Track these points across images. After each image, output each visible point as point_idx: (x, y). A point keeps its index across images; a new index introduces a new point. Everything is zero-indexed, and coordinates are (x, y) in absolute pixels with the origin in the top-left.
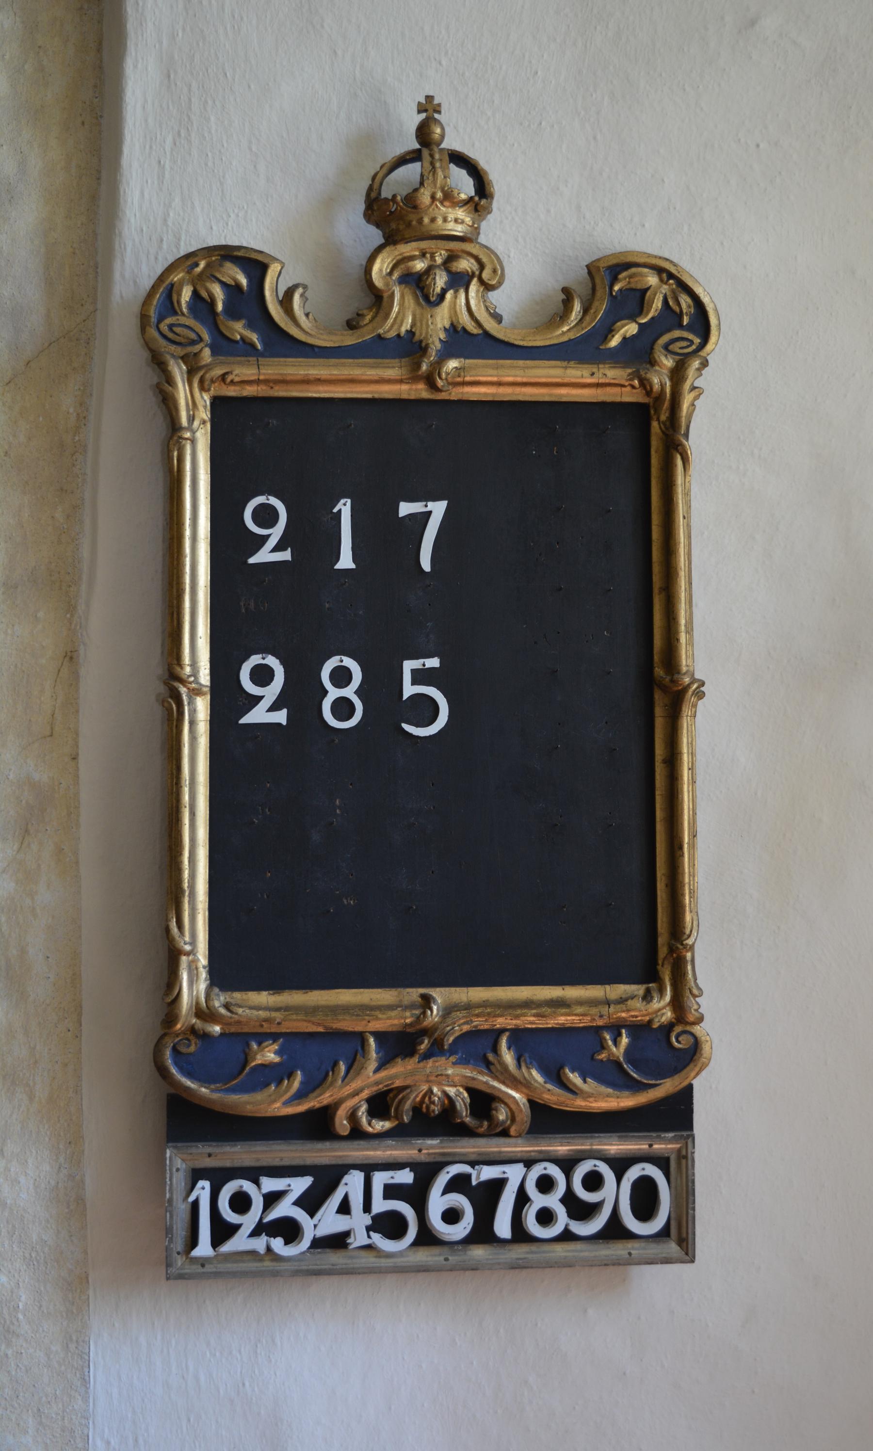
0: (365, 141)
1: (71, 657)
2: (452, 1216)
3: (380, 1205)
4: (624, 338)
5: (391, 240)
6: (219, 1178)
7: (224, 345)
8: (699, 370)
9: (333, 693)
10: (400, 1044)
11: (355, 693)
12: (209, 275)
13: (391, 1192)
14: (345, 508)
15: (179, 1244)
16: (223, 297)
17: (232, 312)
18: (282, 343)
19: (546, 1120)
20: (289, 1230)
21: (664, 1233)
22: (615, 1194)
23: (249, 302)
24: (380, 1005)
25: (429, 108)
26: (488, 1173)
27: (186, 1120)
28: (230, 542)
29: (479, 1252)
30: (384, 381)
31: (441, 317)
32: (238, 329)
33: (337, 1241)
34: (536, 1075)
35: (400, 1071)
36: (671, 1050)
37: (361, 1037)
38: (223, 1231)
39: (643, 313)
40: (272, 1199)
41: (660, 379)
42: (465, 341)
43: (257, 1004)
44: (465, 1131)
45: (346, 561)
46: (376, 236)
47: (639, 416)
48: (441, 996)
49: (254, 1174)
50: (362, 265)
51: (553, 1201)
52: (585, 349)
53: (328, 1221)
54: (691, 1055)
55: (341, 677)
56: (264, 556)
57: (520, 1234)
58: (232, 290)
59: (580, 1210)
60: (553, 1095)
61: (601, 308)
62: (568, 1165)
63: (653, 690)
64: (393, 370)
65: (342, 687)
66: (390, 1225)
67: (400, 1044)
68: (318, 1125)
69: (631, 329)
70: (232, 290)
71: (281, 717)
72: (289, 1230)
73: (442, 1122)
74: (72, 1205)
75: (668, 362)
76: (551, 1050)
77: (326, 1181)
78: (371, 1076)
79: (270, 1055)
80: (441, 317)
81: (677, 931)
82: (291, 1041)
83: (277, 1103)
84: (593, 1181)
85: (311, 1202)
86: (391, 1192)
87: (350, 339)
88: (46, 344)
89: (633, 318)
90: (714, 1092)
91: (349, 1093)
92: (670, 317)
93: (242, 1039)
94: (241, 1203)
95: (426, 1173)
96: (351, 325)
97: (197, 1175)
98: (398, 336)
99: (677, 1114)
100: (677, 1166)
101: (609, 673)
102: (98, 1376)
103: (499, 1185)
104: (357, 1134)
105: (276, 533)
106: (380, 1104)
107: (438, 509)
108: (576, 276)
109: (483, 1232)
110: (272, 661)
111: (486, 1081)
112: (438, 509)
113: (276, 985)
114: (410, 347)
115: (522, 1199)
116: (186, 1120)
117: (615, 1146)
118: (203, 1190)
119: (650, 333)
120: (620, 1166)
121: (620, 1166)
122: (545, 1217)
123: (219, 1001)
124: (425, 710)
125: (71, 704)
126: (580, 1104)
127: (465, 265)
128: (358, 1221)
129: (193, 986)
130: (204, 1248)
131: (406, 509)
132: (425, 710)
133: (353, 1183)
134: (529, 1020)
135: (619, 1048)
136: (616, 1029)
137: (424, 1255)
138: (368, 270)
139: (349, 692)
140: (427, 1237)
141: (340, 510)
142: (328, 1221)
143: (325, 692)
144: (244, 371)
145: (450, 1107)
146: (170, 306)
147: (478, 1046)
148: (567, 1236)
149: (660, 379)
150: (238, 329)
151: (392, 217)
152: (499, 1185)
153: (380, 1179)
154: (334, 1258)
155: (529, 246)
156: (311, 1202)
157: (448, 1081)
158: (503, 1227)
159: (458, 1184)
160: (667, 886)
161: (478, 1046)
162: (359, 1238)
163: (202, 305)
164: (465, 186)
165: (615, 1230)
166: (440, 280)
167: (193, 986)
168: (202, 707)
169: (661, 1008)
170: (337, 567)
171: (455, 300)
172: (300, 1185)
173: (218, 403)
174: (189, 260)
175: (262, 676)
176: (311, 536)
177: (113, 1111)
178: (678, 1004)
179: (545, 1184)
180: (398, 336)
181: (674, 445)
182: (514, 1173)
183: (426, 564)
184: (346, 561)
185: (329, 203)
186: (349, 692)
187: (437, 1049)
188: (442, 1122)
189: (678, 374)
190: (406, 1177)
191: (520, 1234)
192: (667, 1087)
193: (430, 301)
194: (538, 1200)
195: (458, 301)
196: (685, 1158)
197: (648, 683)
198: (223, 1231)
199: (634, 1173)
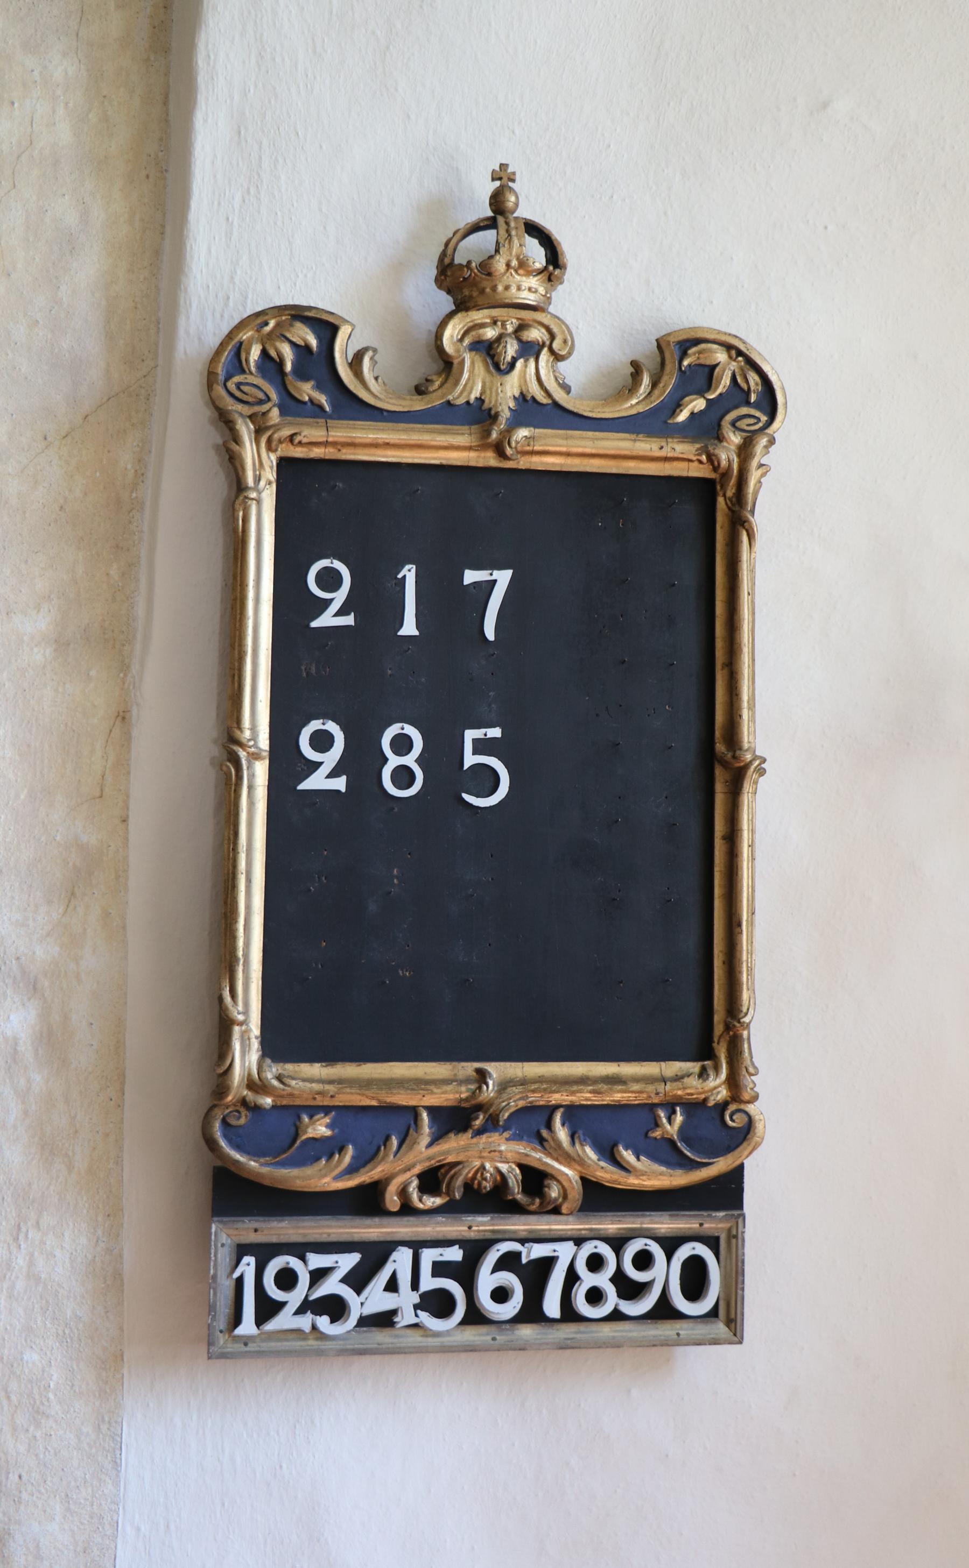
0: (436, 207)
1: (123, 717)
2: (501, 1295)
3: (428, 1283)
4: (692, 413)
5: (462, 306)
6: (264, 1253)
7: (292, 406)
8: (766, 447)
9: (394, 761)
10: (454, 1119)
11: (416, 761)
12: (279, 334)
13: (440, 1269)
14: (409, 574)
15: (222, 1322)
16: (293, 358)
17: (301, 372)
18: (351, 405)
19: (597, 1197)
20: (334, 1308)
21: (713, 1313)
22: (665, 1273)
23: (317, 363)
24: (433, 1080)
25: (503, 176)
26: (539, 1251)
27: (233, 1194)
28: (293, 604)
29: (527, 1331)
30: (453, 448)
31: (511, 386)
32: (307, 390)
33: (385, 1320)
34: (590, 1153)
35: (455, 1147)
36: (723, 1129)
37: (414, 1111)
38: (267, 1309)
39: (713, 388)
40: (318, 1276)
41: (727, 455)
42: (531, 410)
43: (309, 1077)
44: (515, 1209)
45: (409, 628)
46: (445, 302)
47: (704, 491)
48: (496, 1070)
49: (300, 1250)
50: (430, 331)
51: (603, 1280)
52: (654, 423)
53: (375, 1299)
54: (745, 1134)
55: (402, 745)
56: (326, 620)
57: (569, 1314)
58: (302, 350)
60: (606, 1173)
61: (670, 382)
62: (618, 1244)
63: (715, 765)
64: (463, 437)
65: (402, 753)
66: (438, 1304)
67: (454, 1119)
68: (368, 1201)
69: (699, 404)
70: (302, 350)
71: (340, 784)
72: (334, 1308)
73: (495, 1199)
74: (109, 1280)
75: (735, 439)
76: (604, 1126)
77: (374, 1257)
78: (423, 1151)
79: (320, 1128)
80: (511, 386)
81: (733, 1009)
82: (344, 1115)
83: (325, 1178)
84: (643, 1260)
85: (358, 1280)
86: (440, 1269)
87: (418, 404)
88: (105, 399)
89: (701, 393)
90: (762, 1171)
91: (400, 1168)
92: (738, 394)
93: (294, 1112)
94: (287, 1279)
95: (476, 1250)
96: (420, 390)
97: (242, 1250)
98: (468, 403)
99: (727, 1193)
100: (726, 1245)
101: (670, 747)
102: (129, 1457)
103: (547, 1264)
104: (407, 1209)
105: (340, 597)
106: (431, 1180)
107: (503, 578)
108: (645, 350)
109: (532, 1312)
110: (332, 727)
111: (538, 1158)
112: (503, 578)
113: (329, 1058)
114: (480, 415)
115: (572, 1277)
116: (233, 1194)
117: (665, 1224)
118: (248, 1266)
119: (718, 408)
120: (670, 1245)
121: (670, 1245)
122: (595, 1296)
123: (271, 1072)
124: (485, 780)
125: (122, 765)
126: (633, 1182)
127: (536, 334)
128: (406, 1299)
129: (246, 1057)
130: (248, 1326)
131: (470, 576)
132: (485, 780)
133: (401, 1260)
134: (585, 1097)
135: (672, 1126)
136: (670, 1107)
137: (473, 1334)
138: (439, 336)
139: (410, 760)
140: (475, 1316)
141: (405, 576)
142: (375, 1299)
143: (386, 760)
144: (312, 432)
145: (502, 1183)
146: (238, 364)
147: (533, 1122)
148: (616, 1316)
149: (727, 455)
150: (307, 390)
151: (463, 284)
152: (547, 1264)
153: (429, 1256)
154: (380, 1337)
155: (599, 321)
156: (358, 1280)
157: (497, 1156)
158: (552, 1305)
159: (508, 1262)
160: (724, 963)
161: (533, 1122)
162: (407, 1317)
163: (271, 365)
164: (536, 254)
166: (511, 349)
167: (246, 1057)
168: (261, 772)
169: (715, 1087)
170: (401, 633)
171: (524, 372)
172: (348, 1261)
173: (285, 464)
174: (259, 317)
175: (322, 741)
176: (374, 601)
177: (155, 1181)
178: (733, 1082)
179: (595, 1263)
180: (468, 403)
181: (739, 521)
182: (565, 1252)
183: (490, 632)
184: (409, 628)
185: (398, 268)
186: (410, 760)
187: (492, 1124)
188: (495, 1199)
189: (745, 451)
190: (455, 1254)
191: (569, 1314)
192: (721, 1165)
193: (500, 368)
194: (589, 1280)
195: (528, 370)
196: (735, 1237)
197: (708, 758)
199: (684, 1252)
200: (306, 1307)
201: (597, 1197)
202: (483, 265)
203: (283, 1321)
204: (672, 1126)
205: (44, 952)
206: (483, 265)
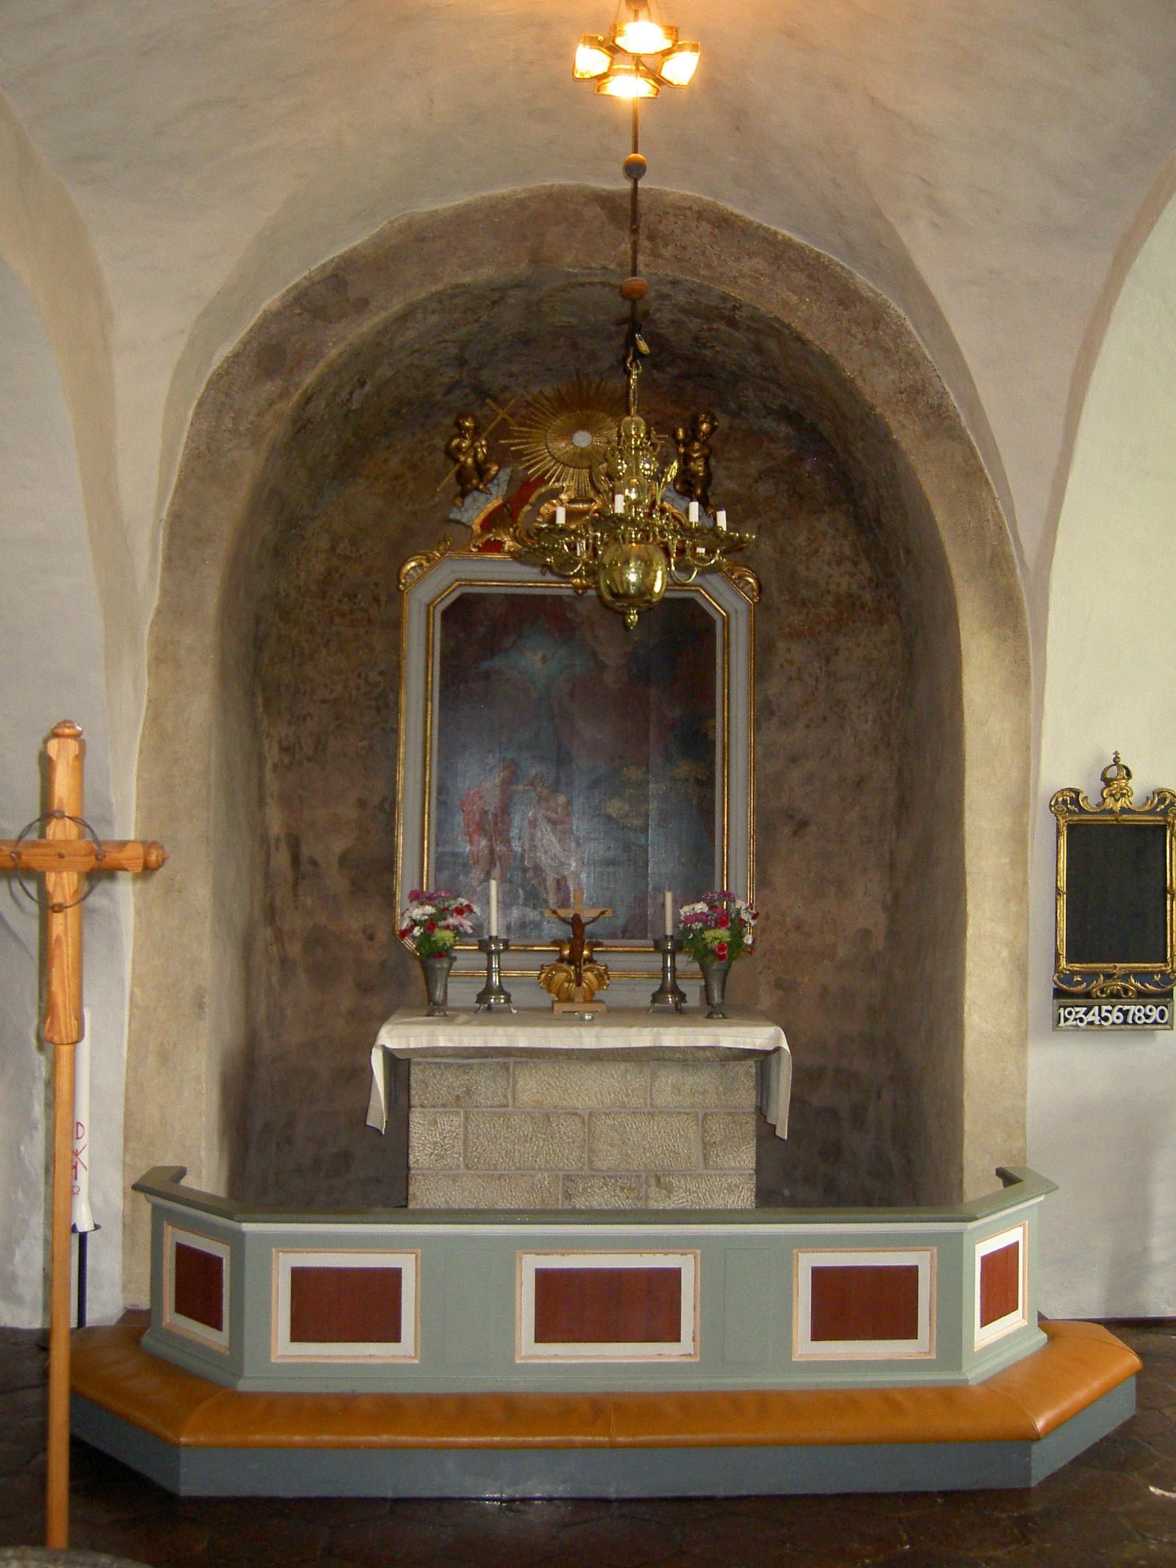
2: (1118, 1018)
16: (1069, 800)
18: (1082, 811)
19: (1141, 994)
20: (1081, 1020)
21: (1166, 1023)
22: (1155, 1014)
23: (1075, 802)
25: (1116, 753)
26: (1125, 1008)
27: (1059, 993)
31: (1119, 804)
33: (1091, 1023)
38: (1066, 1020)
42: (1124, 810)
43: (1077, 966)
46: (1103, 784)
53: (1090, 1018)
57: (1134, 1023)
58: (1071, 798)
59: (1147, 1017)
68: (1088, 995)
70: (1071, 798)
72: (1081, 1020)
76: (1143, 976)
80: (1119, 804)
84: (1151, 1010)
85: (1086, 1014)
93: (1074, 973)
104: (1098, 997)
114: (1111, 812)
119: (1167, 807)
122: (1140, 1018)
129: (1063, 963)
130: (1062, 1023)
142: (1090, 1018)
147: (1125, 977)
151: (1107, 782)
154: (1090, 1027)
155: (1139, 787)
156: (1086, 1014)
159: (1120, 1010)
165: (1155, 1022)
167: (1063, 963)
172: (1085, 1009)
179: (1139, 1011)
182: (1133, 1009)
193: (1117, 801)
194: (1138, 1014)
198: (1066, 1020)
200: (1075, 1019)
201: (1141, 994)
202: (1114, 775)
203: (1068, 1023)
204: (1157, 978)
205: (1010, 937)
206: (1114, 775)
